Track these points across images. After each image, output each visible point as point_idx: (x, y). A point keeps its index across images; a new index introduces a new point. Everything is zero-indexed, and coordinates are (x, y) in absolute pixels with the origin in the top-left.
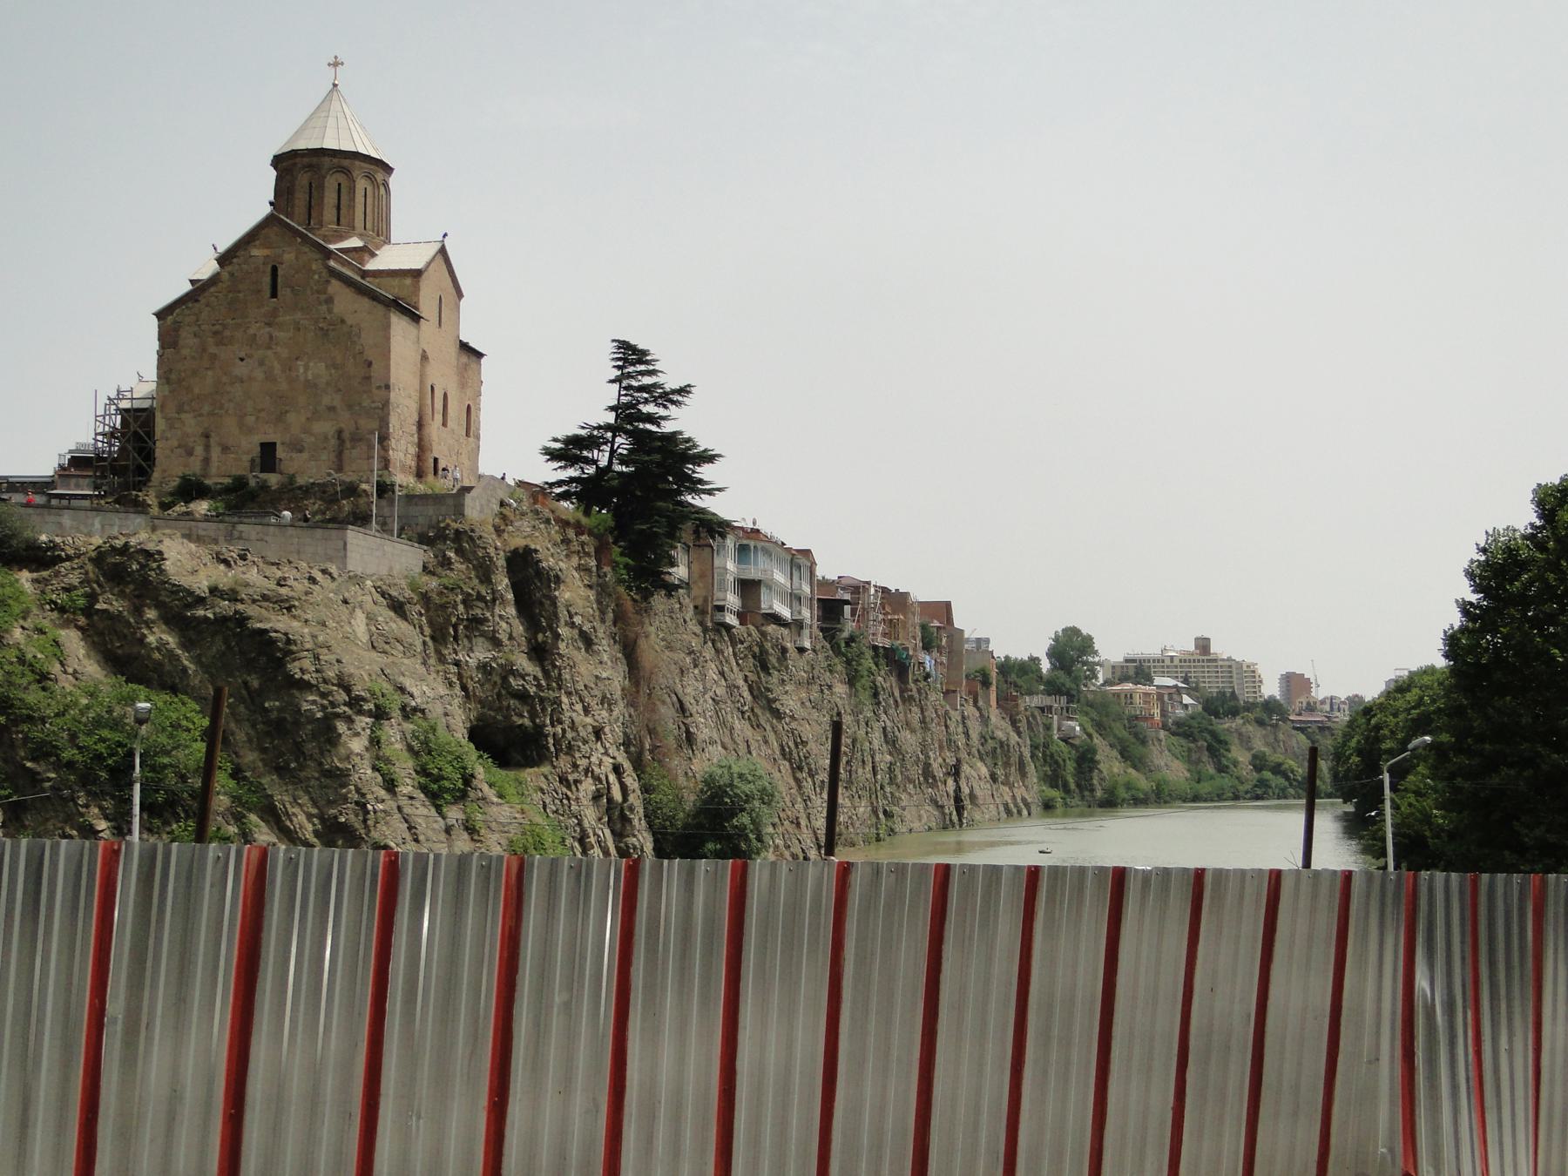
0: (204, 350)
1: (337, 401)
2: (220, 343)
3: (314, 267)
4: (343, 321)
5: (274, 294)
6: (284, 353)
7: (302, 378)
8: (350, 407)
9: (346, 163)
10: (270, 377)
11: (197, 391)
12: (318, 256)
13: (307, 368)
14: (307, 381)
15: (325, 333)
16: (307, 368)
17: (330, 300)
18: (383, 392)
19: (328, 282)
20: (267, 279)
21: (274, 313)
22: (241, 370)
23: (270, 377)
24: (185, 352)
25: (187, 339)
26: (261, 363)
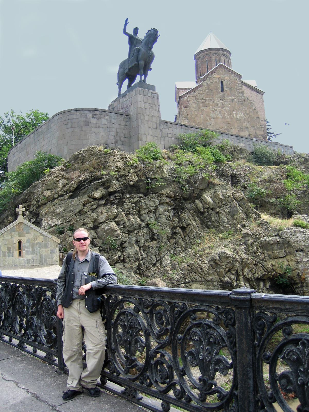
0: (199, 108)
1: (248, 125)
2: (205, 106)
3: (236, 82)
4: (248, 99)
5: (223, 90)
6: (228, 109)
7: (235, 117)
8: (253, 127)
9: (225, 53)
10: (224, 117)
11: (198, 122)
12: (237, 78)
13: (237, 114)
14: (238, 118)
15: (242, 103)
16: (237, 114)
17: (243, 92)
18: (264, 122)
19: (242, 86)
20: (220, 85)
21: (224, 97)
22: (213, 115)
23: (224, 117)
24: (192, 109)
25: (193, 106)
26: (220, 112)
